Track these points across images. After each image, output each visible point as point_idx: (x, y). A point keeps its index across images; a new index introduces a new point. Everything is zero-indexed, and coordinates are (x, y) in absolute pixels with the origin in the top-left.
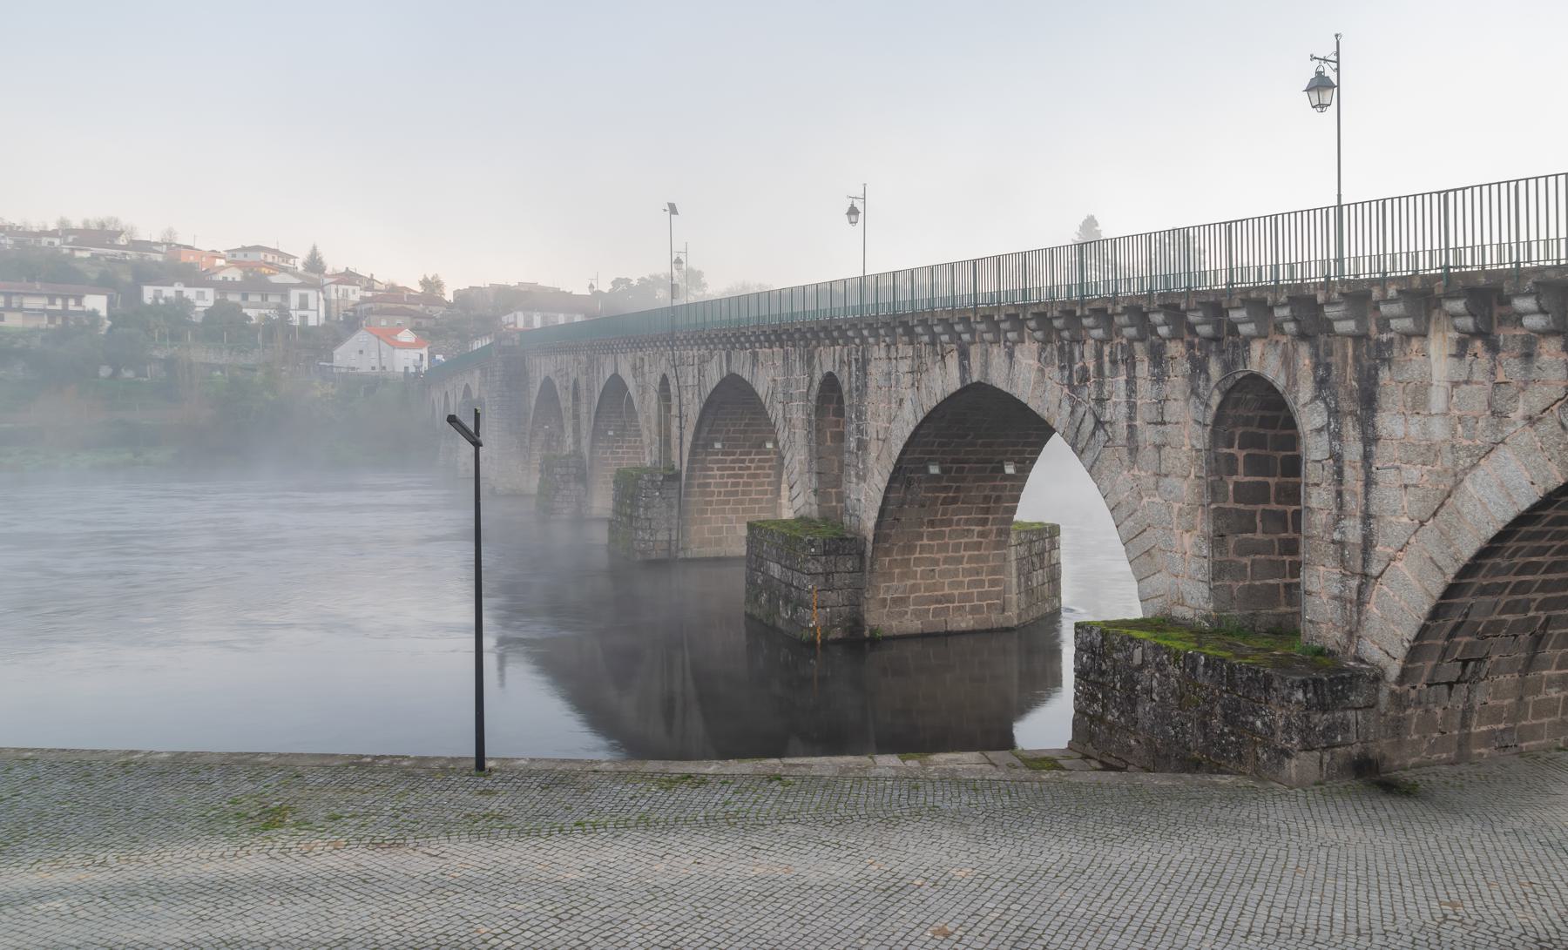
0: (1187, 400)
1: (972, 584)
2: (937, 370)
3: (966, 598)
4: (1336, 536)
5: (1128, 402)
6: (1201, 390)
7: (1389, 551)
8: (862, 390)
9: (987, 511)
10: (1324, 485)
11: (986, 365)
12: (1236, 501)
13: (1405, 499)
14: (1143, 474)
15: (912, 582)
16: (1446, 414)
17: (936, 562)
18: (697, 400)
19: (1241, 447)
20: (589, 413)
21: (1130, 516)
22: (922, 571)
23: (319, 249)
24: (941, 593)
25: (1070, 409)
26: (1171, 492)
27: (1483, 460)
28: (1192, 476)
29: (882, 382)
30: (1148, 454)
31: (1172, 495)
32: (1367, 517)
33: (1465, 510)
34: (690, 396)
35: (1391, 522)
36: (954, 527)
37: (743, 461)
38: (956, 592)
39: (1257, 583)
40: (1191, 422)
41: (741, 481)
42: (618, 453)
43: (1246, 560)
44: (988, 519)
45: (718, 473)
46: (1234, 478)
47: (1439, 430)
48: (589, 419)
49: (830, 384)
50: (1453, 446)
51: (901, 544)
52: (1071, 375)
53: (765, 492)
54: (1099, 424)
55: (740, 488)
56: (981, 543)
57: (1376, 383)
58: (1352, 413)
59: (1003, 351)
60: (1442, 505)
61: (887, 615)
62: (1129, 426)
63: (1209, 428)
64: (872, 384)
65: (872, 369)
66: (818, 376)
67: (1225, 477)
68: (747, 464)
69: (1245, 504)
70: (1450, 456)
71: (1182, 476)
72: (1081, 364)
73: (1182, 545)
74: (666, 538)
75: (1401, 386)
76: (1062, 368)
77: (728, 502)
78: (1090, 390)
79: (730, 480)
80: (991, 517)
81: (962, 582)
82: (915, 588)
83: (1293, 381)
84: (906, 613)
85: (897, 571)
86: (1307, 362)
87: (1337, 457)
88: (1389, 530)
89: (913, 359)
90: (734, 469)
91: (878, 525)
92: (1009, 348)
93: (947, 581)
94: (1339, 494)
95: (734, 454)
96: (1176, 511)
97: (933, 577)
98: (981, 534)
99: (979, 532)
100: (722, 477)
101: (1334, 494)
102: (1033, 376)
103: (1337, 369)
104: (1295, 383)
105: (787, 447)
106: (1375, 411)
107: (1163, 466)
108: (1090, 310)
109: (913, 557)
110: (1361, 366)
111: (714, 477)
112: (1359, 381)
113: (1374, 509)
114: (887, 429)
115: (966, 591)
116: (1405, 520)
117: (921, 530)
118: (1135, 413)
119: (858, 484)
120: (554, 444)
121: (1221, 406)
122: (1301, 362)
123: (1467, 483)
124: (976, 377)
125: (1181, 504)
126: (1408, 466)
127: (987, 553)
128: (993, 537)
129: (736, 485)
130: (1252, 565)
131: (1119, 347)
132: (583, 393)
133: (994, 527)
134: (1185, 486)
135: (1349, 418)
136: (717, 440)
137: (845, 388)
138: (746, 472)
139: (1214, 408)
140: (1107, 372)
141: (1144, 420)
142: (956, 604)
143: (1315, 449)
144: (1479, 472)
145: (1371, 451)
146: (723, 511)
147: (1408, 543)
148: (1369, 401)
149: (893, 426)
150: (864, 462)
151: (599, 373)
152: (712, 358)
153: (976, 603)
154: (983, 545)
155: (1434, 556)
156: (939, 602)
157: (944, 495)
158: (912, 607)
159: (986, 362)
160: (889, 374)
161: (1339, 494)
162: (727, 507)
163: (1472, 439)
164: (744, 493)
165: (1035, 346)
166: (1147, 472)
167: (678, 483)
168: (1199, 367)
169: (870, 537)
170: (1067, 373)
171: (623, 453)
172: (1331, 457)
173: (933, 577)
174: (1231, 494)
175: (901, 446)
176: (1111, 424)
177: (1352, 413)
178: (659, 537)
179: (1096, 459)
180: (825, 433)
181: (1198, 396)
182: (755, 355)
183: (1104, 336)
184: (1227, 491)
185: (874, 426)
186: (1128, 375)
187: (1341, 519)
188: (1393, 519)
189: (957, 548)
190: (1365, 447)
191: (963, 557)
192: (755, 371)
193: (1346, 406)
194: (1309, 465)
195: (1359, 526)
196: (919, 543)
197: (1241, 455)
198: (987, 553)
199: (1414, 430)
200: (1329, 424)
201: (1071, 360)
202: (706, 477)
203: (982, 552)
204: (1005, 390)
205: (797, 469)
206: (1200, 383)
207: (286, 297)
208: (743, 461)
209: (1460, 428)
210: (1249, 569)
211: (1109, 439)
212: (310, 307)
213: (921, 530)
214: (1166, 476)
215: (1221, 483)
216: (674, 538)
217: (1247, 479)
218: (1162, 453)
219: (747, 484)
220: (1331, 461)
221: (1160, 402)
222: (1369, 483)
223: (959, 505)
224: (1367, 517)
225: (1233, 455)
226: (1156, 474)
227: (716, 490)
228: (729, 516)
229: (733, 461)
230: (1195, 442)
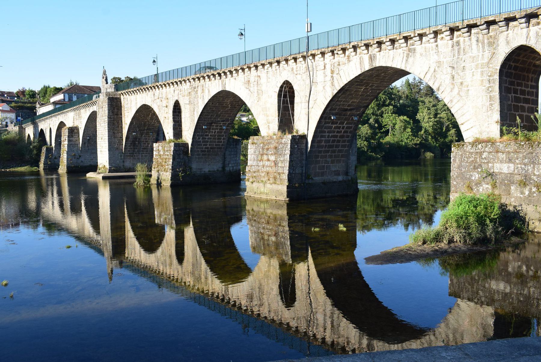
37: (339, 128)
42: (206, 138)
45: (327, 134)
53: (344, 146)
55: (335, 144)
74: (300, 171)
77: (328, 151)
79: (332, 139)
90: (334, 132)
105: (455, 101)
120: (137, 143)
162: (328, 154)
164: (337, 146)
171: (208, 138)
192: (411, 60)
202: (322, 136)
216: (304, 172)
228: (328, 159)
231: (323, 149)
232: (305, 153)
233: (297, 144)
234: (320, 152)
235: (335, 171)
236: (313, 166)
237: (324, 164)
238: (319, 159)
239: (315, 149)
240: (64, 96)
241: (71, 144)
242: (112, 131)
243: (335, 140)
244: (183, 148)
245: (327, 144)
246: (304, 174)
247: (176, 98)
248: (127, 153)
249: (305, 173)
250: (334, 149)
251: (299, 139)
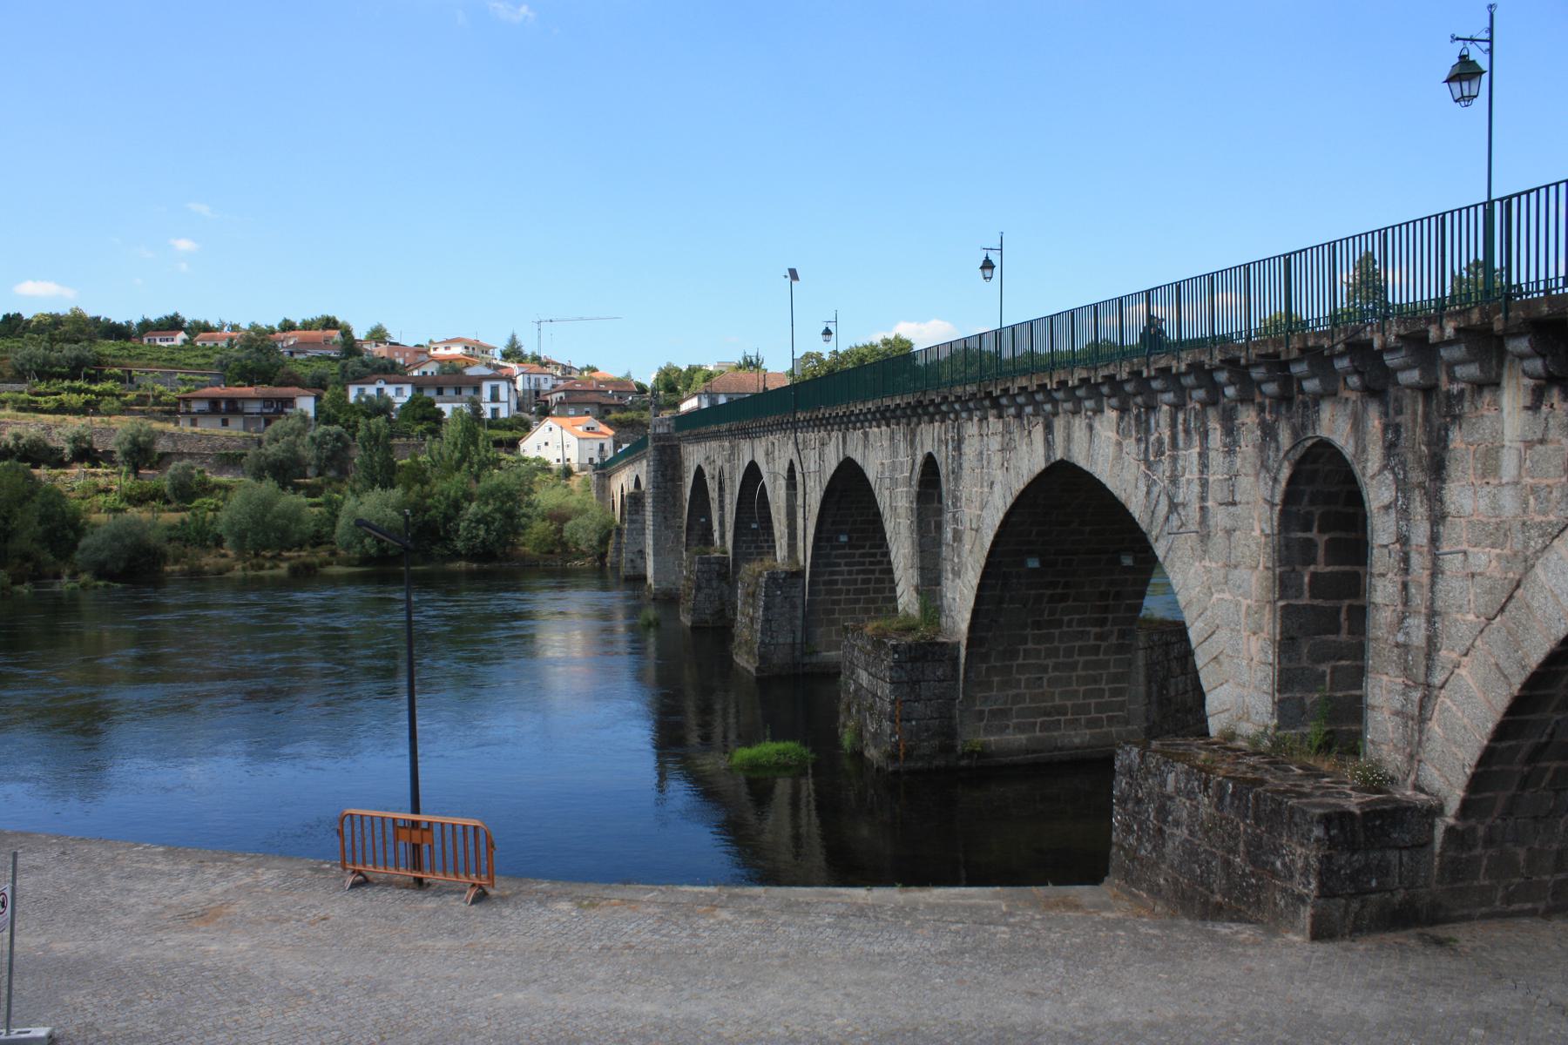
0: (1257, 475)
1: (1087, 694)
2: (1024, 447)
3: (1081, 709)
4: (1401, 638)
5: (1200, 478)
6: (1271, 462)
7: (1454, 656)
8: (956, 473)
9: (1106, 609)
10: (1390, 575)
11: (1068, 439)
12: (1313, 596)
13: (1472, 591)
14: (1214, 565)
15: (1015, 691)
16: (1517, 483)
17: (1045, 669)
18: (818, 488)
19: (1321, 531)
20: (732, 503)
21: (1200, 616)
22: (1027, 679)
23: (518, 338)
24: (1050, 704)
25: (1145, 489)
26: (1240, 587)
27: (1556, 541)
28: (1261, 567)
29: (975, 463)
30: (1218, 539)
31: (1241, 591)
32: (1432, 615)
33: (1535, 604)
34: (812, 484)
35: (1457, 620)
36: (1065, 629)
37: (874, 555)
38: (1069, 703)
39: (1339, 694)
40: (1261, 502)
41: (872, 577)
43: (1326, 668)
44: (1106, 618)
45: (846, 568)
46: (1312, 568)
47: (1509, 503)
48: (732, 513)
49: (930, 463)
50: (1524, 524)
51: (1001, 648)
52: (1147, 449)
54: (1173, 507)
55: (872, 586)
56: (1099, 646)
57: (1446, 447)
58: (1421, 485)
59: (1085, 422)
60: (1510, 597)
61: (985, 729)
62: (1202, 508)
63: (1278, 508)
64: (966, 465)
65: (966, 448)
66: (919, 459)
67: (1298, 568)
68: (879, 558)
69: (1325, 599)
70: (1520, 536)
71: (1251, 567)
72: (1156, 435)
73: (1249, 650)
74: (789, 640)
75: (1472, 448)
76: (1139, 440)
77: (857, 601)
78: (1165, 467)
79: (860, 577)
80: (1110, 616)
81: (1077, 691)
82: (1018, 699)
83: (1361, 448)
84: (1007, 727)
85: (996, 679)
86: (1376, 422)
87: (1403, 540)
88: (1453, 630)
89: (1003, 436)
90: (863, 564)
91: (973, 627)
92: (1090, 418)
93: (1058, 690)
94: (1405, 586)
95: (863, 547)
96: (1244, 609)
97: (1040, 686)
98: (1100, 637)
99: (1096, 634)
100: (850, 573)
101: (1400, 587)
102: (1111, 451)
103: (1407, 430)
104: (1364, 450)
106: (1444, 481)
107: (1232, 556)
108: (1156, 369)
109: (1015, 663)
110: (1431, 427)
111: (841, 573)
112: (1428, 445)
113: (1439, 604)
114: (979, 516)
115: (1081, 701)
116: (1471, 617)
117: (1026, 632)
118: (1207, 492)
119: (953, 581)
121: (1292, 481)
122: (1370, 425)
123: (1539, 570)
124: (1059, 455)
125: (1249, 601)
126: (1476, 550)
127: (1107, 658)
128: (1113, 640)
129: (864, 581)
130: (1332, 672)
131: (1193, 414)
132: (727, 483)
133: (1116, 629)
134: (1254, 580)
135: (1417, 492)
136: (842, 532)
137: (943, 471)
138: (878, 567)
139: (1283, 484)
140: (1181, 444)
141: (1215, 500)
142: (1069, 717)
143: (1382, 530)
144: (1552, 556)
145: (1438, 532)
146: (854, 611)
147: (1473, 645)
148: (1437, 467)
149: (984, 514)
150: (959, 556)
151: (739, 459)
152: (830, 440)
153: (1093, 715)
154: (1102, 649)
155: (1501, 662)
156: (1049, 714)
157: (1049, 592)
158: (1015, 721)
159: (1069, 435)
160: (981, 453)
161: (1405, 586)
163: (1545, 513)
164: (876, 591)
165: (1114, 415)
166: (1217, 563)
167: (802, 581)
168: (1268, 432)
169: (964, 642)
170: (1143, 446)
172: (1398, 541)
173: (1040, 686)
174: (1306, 587)
175: (991, 538)
176: (1184, 505)
177: (1421, 485)
178: (781, 640)
179: (1170, 549)
180: (929, 522)
181: (1268, 471)
182: (866, 435)
183: (1175, 400)
184: (1301, 584)
185: (968, 513)
186: (1201, 445)
187: (1405, 618)
188: (1459, 616)
189: (1069, 652)
190: (1432, 526)
191: (1077, 663)
193: (1416, 476)
194: (1375, 551)
195: (1424, 626)
196: (1022, 647)
197: (1321, 539)
198: (1107, 658)
199: (1483, 504)
200: (1397, 499)
201: (1148, 431)
203: (1101, 657)
204: (1085, 468)
205: (902, 564)
206: (1271, 453)
207: (478, 389)
208: (874, 555)
209: (1532, 500)
210: (1328, 678)
211: (1183, 525)
212: (501, 399)
213: (1026, 632)
214: (1236, 567)
215: (1293, 575)
216: (798, 641)
217: (1329, 569)
218: (1232, 539)
220: (1398, 546)
221: (1231, 479)
222: (1435, 572)
223: (1070, 603)
224: (1432, 615)
225: (1310, 540)
226: (1226, 565)
227: (844, 587)
229: (862, 555)
230: (1264, 526)
232: (800, 607)
233: (781, 589)
234: (837, 602)
236: (822, 629)
238: (837, 616)
239: (822, 597)
240: (700, 400)
241: (635, 529)
242: (660, 514)
243: (870, 579)
244: (717, 567)
245: (852, 587)
246: (798, 646)
247: (720, 464)
249: (802, 643)
251: (784, 579)
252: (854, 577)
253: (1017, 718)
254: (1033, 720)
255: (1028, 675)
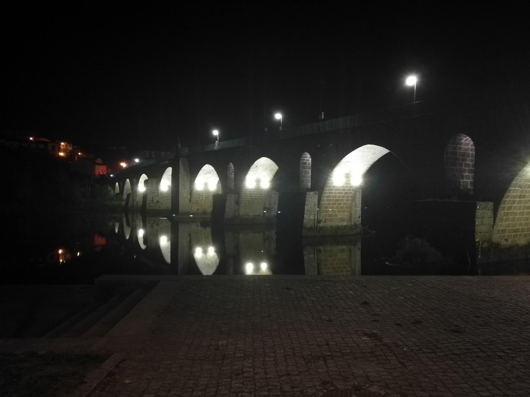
15: (509, 222)
36: (526, 199)
77: (335, 204)
85: (505, 217)
142: (520, 233)
156: (515, 232)
213: (516, 199)
216: (316, 218)
219: (343, 197)
231: (331, 202)
235: (340, 218)
237: (331, 213)
245: (335, 199)
246: (316, 220)
248: (194, 200)
250: (340, 202)
252: (336, 195)
253: (508, 233)
254: (511, 234)
255: (512, 217)
